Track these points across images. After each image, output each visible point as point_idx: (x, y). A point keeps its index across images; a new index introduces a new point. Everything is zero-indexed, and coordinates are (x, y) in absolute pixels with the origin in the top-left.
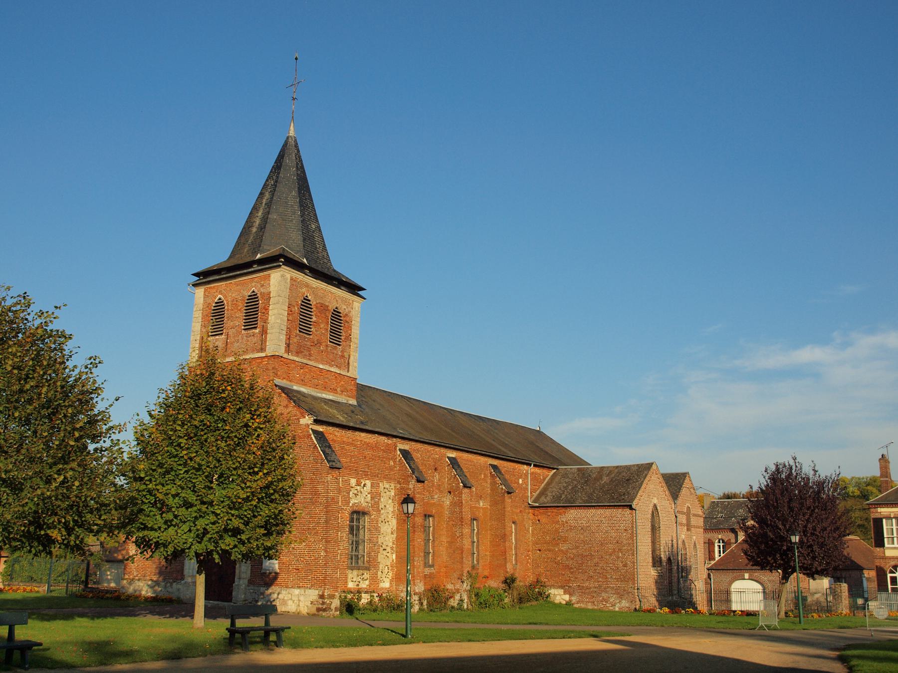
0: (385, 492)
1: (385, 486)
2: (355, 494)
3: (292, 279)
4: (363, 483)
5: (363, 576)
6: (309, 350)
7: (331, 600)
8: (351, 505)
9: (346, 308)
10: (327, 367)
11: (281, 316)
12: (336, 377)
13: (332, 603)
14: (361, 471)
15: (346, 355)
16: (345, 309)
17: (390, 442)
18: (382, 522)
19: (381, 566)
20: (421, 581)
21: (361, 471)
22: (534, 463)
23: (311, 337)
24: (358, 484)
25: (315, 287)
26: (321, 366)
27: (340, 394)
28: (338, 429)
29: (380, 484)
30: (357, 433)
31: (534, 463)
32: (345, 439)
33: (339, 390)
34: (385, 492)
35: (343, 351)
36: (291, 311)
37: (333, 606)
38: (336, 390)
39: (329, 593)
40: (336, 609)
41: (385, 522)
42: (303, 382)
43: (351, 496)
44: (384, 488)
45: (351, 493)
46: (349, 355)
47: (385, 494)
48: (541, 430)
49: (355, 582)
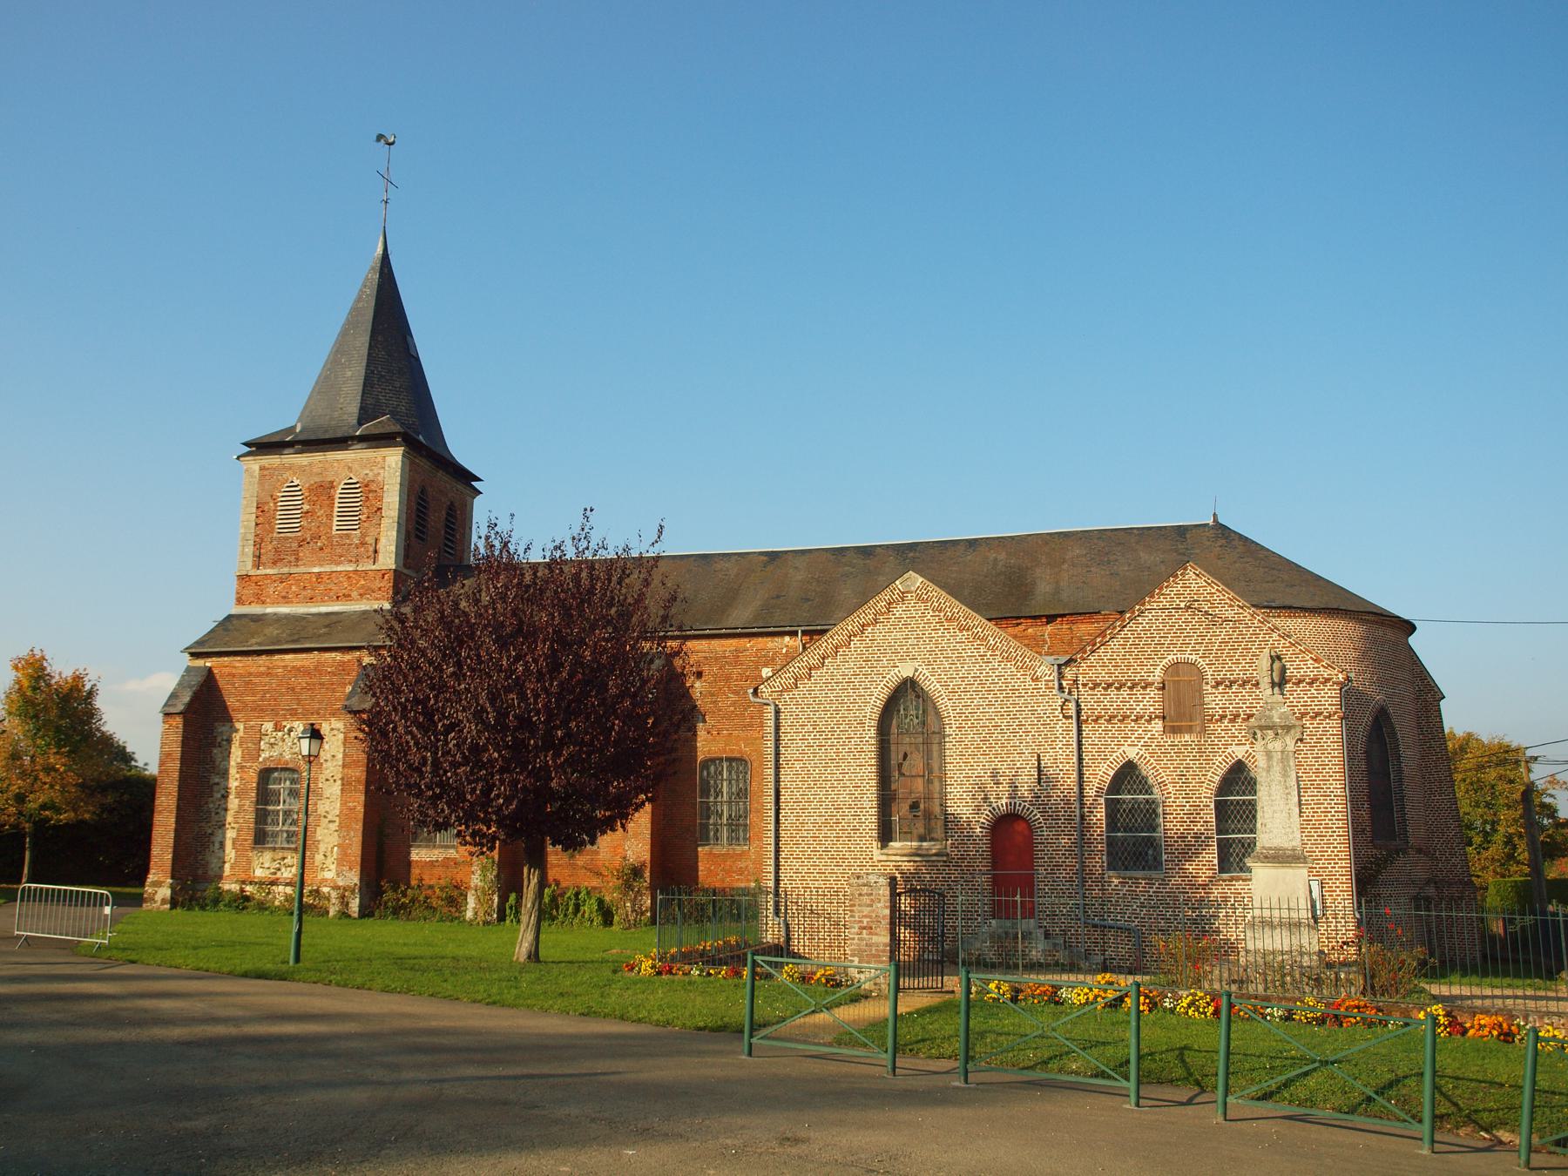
0: (334, 735)
1: (332, 726)
2: (271, 744)
3: (262, 468)
4: (288, 726)
5: (286, 861)
6: (296, 553)
7: (156, 889)
8: (261, 759)
9: (367, 472)
10: (327, 569)
11: (245, 523)
12: (350, 577)
13: (156, 892)
14: (283, 710)
15: (370, 540)
16: (366, 474)
17: (347, 657)
18: (327, 780)
19: (322, 848)
20: (351, 869)
21: (283, 710)
22: (803, 628)
23: (299, 534)
24: (278, 728)
25: (306, 463)
26: (316, 570)
27: (358, 600)
28: (239, 658)
29: (323, 725)
30: (277, 657)
31: (803, 628)
32: (252, 670)
33: (355, 594)
34: (334, 735)
35: (364, 535)
36: (262, 511)
37: (158, 897)
38: (349, 596)
39: (156, 879)
40: (164, 901)
41: (335, 781)
42: (285, 599)
43: (262, 748)
44: (332, 729)
45: (262, 743)
46: (376, 540)
47: (333, 738)
48: (1221, 521)
49: (269, 868)
